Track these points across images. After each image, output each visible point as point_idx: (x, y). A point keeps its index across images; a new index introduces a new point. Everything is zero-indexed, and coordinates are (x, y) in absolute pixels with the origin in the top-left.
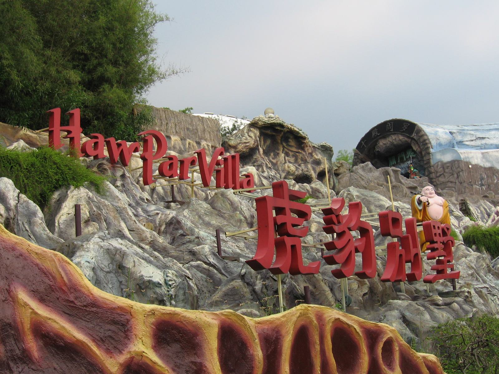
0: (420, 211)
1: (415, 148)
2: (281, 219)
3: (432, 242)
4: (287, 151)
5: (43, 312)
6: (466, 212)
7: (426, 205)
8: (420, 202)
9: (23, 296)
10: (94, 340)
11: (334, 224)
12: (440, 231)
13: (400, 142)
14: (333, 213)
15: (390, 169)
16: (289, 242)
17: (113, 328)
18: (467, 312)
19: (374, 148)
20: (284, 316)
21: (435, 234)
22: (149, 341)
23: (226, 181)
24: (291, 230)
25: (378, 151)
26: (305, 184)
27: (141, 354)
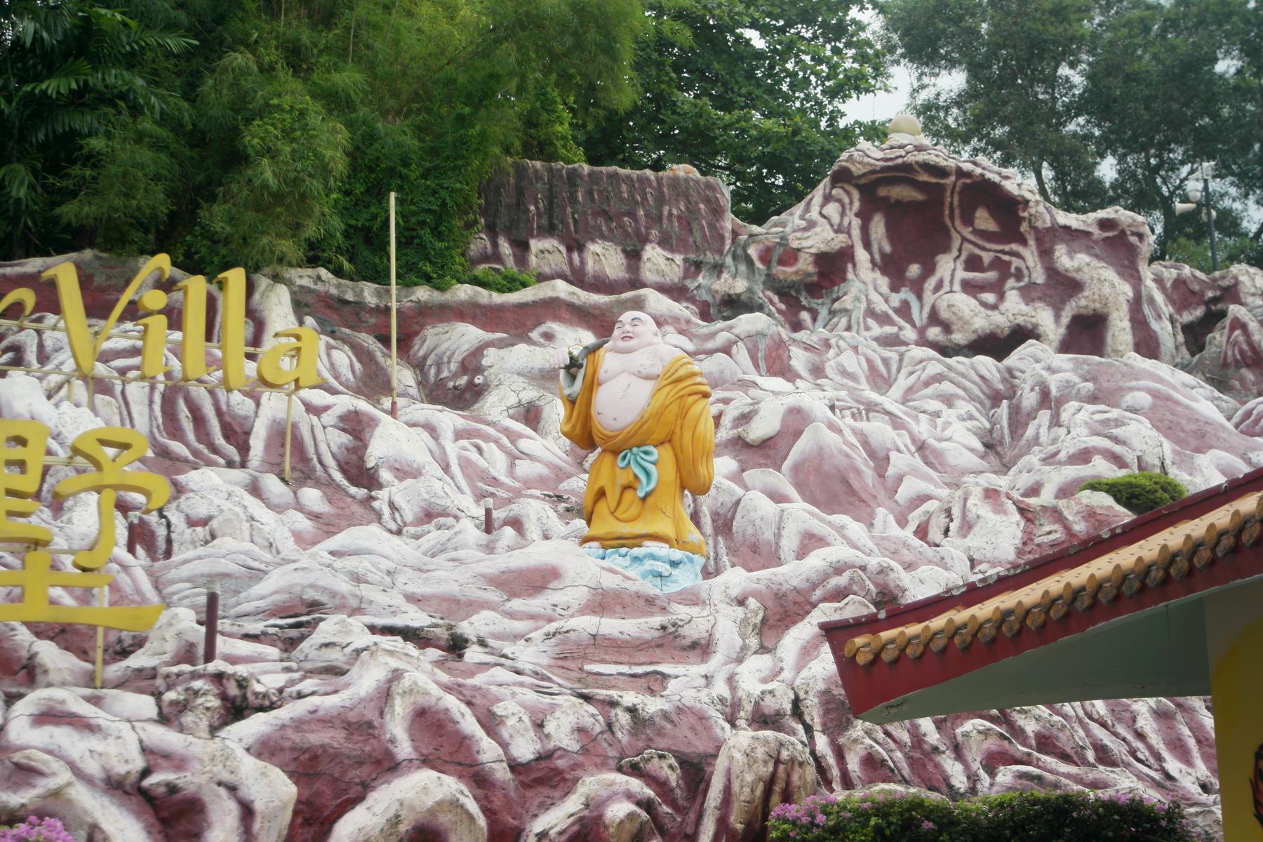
4: (977, 251)
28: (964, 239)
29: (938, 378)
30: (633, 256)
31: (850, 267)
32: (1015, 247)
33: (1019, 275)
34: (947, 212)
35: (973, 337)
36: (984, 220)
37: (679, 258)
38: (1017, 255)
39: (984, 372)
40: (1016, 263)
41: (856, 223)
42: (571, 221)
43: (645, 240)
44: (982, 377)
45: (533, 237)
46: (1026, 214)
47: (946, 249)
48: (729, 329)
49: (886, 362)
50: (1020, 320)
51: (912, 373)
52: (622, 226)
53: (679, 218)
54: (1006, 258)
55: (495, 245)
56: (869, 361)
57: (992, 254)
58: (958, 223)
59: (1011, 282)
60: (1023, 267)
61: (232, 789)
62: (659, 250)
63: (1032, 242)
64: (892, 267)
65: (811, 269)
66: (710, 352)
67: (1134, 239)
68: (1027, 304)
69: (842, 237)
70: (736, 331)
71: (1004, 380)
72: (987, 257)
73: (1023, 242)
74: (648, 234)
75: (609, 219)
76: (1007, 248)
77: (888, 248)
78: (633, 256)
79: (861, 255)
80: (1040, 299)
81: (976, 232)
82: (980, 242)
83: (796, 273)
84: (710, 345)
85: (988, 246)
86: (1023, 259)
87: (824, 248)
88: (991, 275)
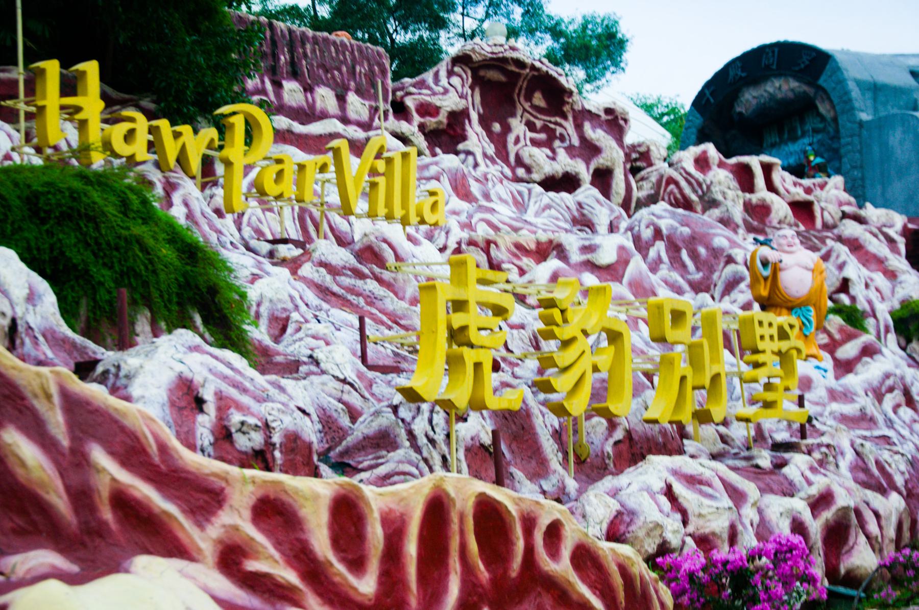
0: (766, 279)
1: (823, 108)
2: (458, 320)
3: (756, 351)
4: (532, 119)
5: (125, 477)
8: (765, 263)
10: (184, 511)
12: (774, 331)
13: (790, 95)
14: (557, 306)
15: (754, 162)
16: (470, 356)
17: (206, 497)
18: (809, 483)
19: (732, 106)
20: (413, 487)
22: (247, 514)
23: (389, 204)
24: (474, 336)
25: (740, 114)
26: (564, 195)
27: (236, 528)
28: (525, 110)
29: (548, 207)
30: (341, 99)
31: (467, 122)
32: (558, 120)
33: (562, 138)
34: (517, 91)
35: (543, 177)
36: (538, 99)
37: (367, 103)
38: (561, 125)
39: (568, 204)
40: (559, 130)
41: (470, 92)
42: (306, 70)
43: (347, 89)
44: (568, 207)
45: (284, 79)
46: (570, 100)
47: (513, 115)
48: (436, 164)
49: (520, 193)
50: (568, 169)
51: (536, 202)
52: (333, 77)
53: (365, 75)
54: (552, 126)
55: (263, 82)
56: (511, 193)
57: (542, 122)
58: (522, 99)
59: (557, 143)
60: (565, 133)
61: (868, 504)
62: (356, 97)
63: (570, 118)
64: (485, 122)
65: (445, 121)
66: (428, 179)
67: (622, 122)
68: (571, 159)
69: (464, 101)
70: (443, 166)
71: (577, 210)
72: (539, 124)
73: (565, 117)
74: (349, 84)
75: (327, 71)
76: (553, 119)
77: (481, 111)
78: (341, 99)
79: (474, 116)
80: (579, 156)
81: (534, 107)
82: (534, 113)
83: (436, 123)
84: (426, 174)
85: (539, 116)
86: (565, 129)
87: (455, 108)
88: (542, 136)
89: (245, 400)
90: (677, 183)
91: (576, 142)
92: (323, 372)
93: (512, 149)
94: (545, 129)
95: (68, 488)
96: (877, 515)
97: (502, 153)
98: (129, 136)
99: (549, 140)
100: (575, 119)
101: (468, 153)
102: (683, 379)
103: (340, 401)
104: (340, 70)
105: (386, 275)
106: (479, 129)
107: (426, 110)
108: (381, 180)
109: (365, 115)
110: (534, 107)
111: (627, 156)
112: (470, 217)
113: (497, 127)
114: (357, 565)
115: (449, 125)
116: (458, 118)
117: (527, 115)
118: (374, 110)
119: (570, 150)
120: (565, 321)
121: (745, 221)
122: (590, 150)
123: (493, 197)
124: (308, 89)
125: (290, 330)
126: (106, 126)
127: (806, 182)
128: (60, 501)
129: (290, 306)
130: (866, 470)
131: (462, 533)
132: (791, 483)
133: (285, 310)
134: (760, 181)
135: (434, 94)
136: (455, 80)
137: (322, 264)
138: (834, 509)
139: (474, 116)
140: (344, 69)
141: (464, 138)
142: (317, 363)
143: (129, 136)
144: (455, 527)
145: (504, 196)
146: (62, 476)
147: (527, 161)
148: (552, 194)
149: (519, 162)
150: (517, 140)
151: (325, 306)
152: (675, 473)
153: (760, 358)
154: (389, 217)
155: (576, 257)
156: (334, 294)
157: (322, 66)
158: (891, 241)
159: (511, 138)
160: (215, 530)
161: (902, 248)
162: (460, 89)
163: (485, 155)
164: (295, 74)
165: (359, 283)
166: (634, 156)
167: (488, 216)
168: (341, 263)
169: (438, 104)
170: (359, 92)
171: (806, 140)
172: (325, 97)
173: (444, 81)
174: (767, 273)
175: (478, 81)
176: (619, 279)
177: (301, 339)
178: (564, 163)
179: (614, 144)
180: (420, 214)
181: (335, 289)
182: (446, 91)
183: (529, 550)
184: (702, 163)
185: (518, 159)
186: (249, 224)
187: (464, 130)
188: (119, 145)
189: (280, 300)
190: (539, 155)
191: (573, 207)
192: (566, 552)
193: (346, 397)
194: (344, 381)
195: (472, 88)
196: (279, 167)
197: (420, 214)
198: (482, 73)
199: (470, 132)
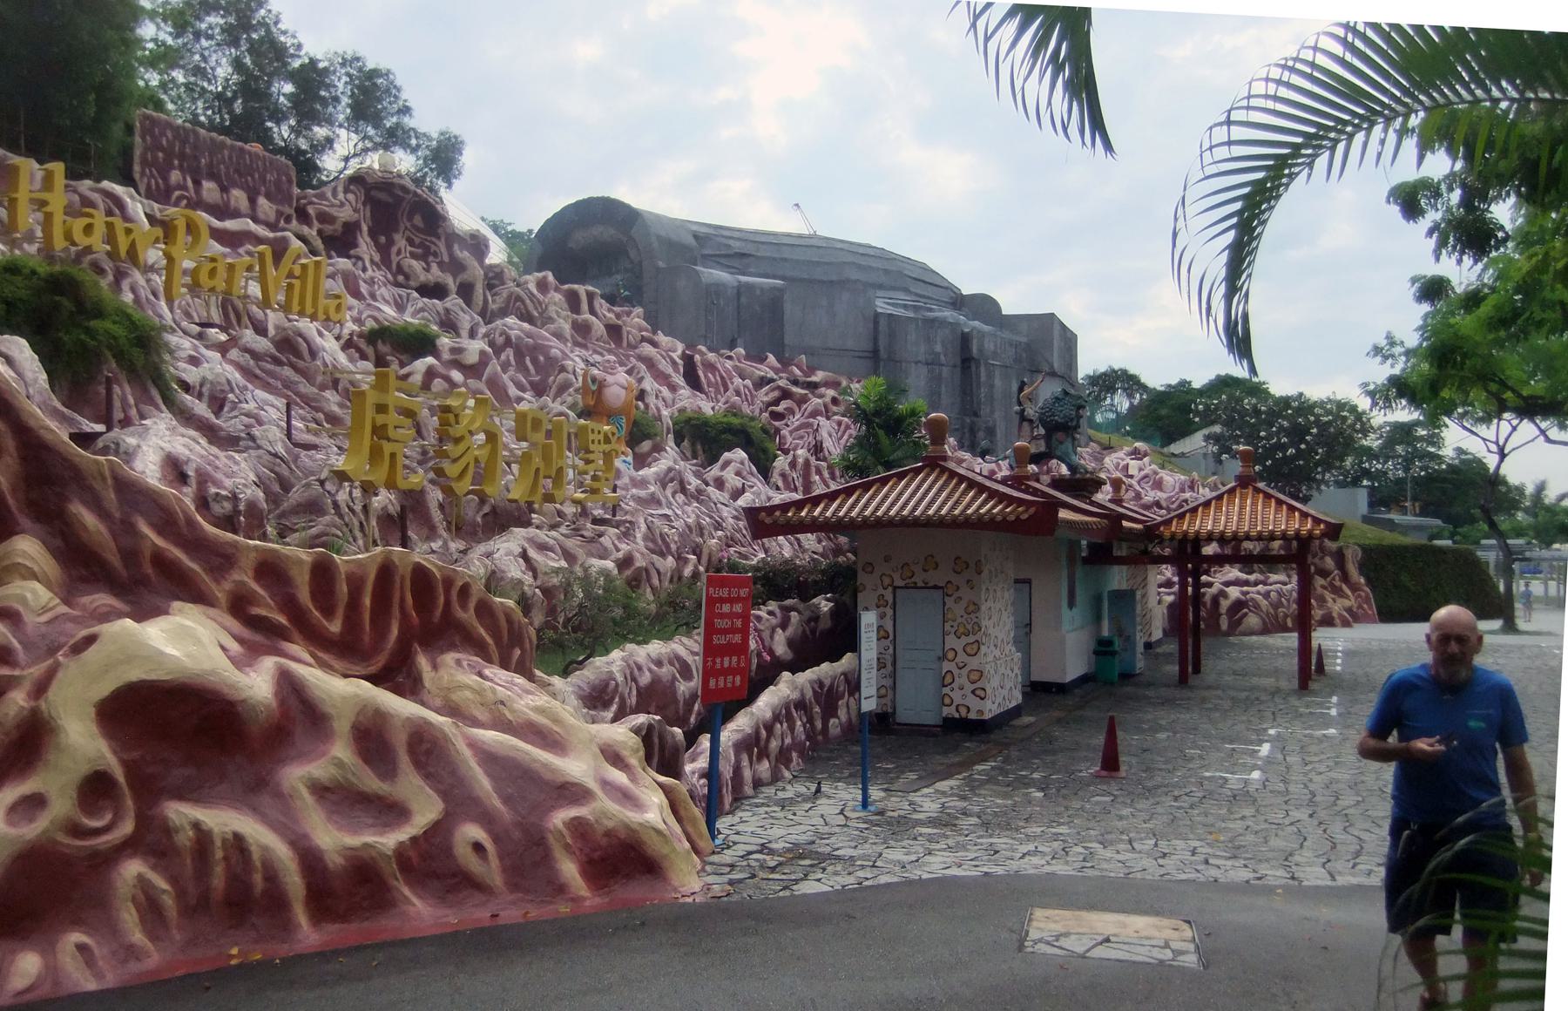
0: (593, 392)
1: (633, 254)
2: (380, 419)
3: (588, 451)
5: (160, 542)
6: (693, 382)
7: (602, 385)
9: (145, 529)
10: (204, 570)
11: (450, 425)
12: (601, 437)
15: (581, 289)
16: (388, 448)
18: (618, 550)
21: (593, 442)
22: (251, 573)
23: (302, 302)
24: (391, 433)
27: (243, 583)
29: (422, 310)
33: (435, 255)
37: (274, 207)
40: (433, 248)
43: (258, 193)
47: (397, 231)
49: (400, 296)
55: (185, 179)
59: (431, 258)
64: (373, 234)
72: (417, 240)
73: (439, 238)
75: (241, 175)
78: (252, 201)
79: (365, 228)
87: (348, 219)
88: (420, 251)
89: (219, 476)
90: (523, 302)
91: (446, 259)
92: (259, 447)
93: (395, 259)
94: (421, 245)
95: (120, 550)
96: (659, 573)
97: (386, 261)
98: (88, 229)
99: (425, 255)
100: (446, 240)
101: (359, 258)
102: (537, 470)
103: (272, 471)
104: (253, 177)
105: (301, 364)
106: (368, 240)
107: (324, 218)
108: (297, 283)
109: (272, 217)
110: (414, 226)
111: (486, 275)
112: (360, 313)
113: (383, 239)
114: (328, 612)
115: (344, 233)
116: (351, 229)
117: (407, 232)
118: (279, 214)
119: (441, 264)
120: (457, 423)
121: (572, 336)
122: (456, 267)
123: (379, 298)
124: (224, 189)
125: (226, 409)
126: (68, 218)
127: (617, 309)
128: (114, 559)
129: (227, 388)
130: (654, 541)
131: (402, 588)
132: (606, 549)
133: (223, 391)
134: (585, 306)
135: (333, 206)
136: (351, 197)
137: (246, 350)
138: (633, 568)
139: (365, 228)
140: (257, 176)
141: (356, 246)
142: (252, 438)
143: (88, 229)
144: (397, 585)
145: (387, 298)
146: (115, 539)
147: (406, 269)
148: (425, 300)
149: (400, 270)
150: (399, 253)
151: (250, 386)
152: (531, 540)
153: (591, 457)
154: (301, 313)
155: (446, 356)
156: (256, 377)
157: (237, 171)
158: (674, 363)
159: (394, 250)
160: (227, 586)
161: (682, 370)
162: (354, 204)
163: (372, 262)
164: (213, 176)
165: (278, 369)
166: (491, 275)
167: (376, 314)
168: (263, 351)
169: (336, 214)
170: (268, 197)
171: (619, 277)
172: (238, 197)
173: (341, 196)
174: (594, 388)
175: (369, 200)
176: (479, 377)
177: (236, 417)
178: (436, 274)
179: (476, 264)
180: (326, 313)
181: (258, 372)
182: (342, 205)
183: (448, 603)
184: (543, 286)
185: (399, 265)
186: (179, 307)
187: (356, 238)
188: (78, 235)
189: (219, 383)
190: (417, 265)
191: (442, 312)
192: (472, 605)
193: (277, 469)
194: (276, 455)
195: (364, 204)
196: (213, 265)
197: (326, 313)
198: (373, 193)
199: (360, 240)
